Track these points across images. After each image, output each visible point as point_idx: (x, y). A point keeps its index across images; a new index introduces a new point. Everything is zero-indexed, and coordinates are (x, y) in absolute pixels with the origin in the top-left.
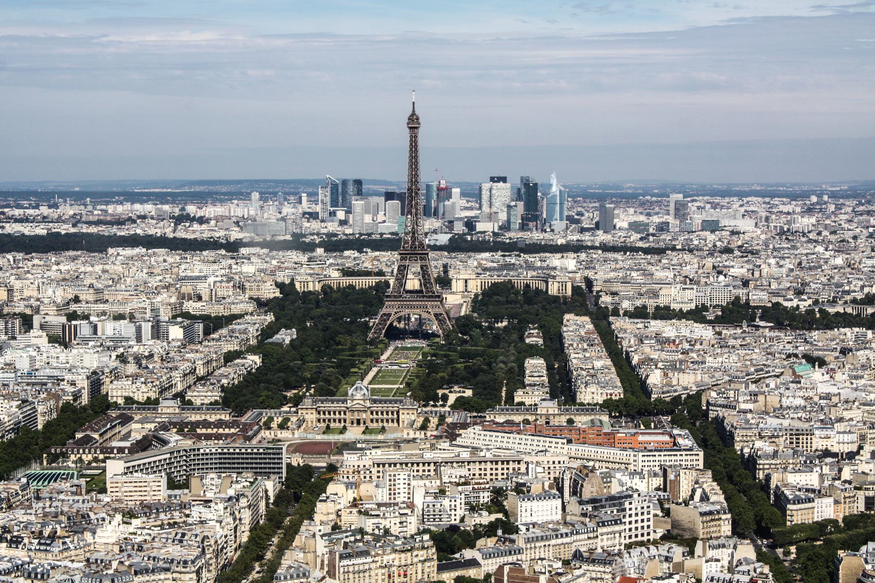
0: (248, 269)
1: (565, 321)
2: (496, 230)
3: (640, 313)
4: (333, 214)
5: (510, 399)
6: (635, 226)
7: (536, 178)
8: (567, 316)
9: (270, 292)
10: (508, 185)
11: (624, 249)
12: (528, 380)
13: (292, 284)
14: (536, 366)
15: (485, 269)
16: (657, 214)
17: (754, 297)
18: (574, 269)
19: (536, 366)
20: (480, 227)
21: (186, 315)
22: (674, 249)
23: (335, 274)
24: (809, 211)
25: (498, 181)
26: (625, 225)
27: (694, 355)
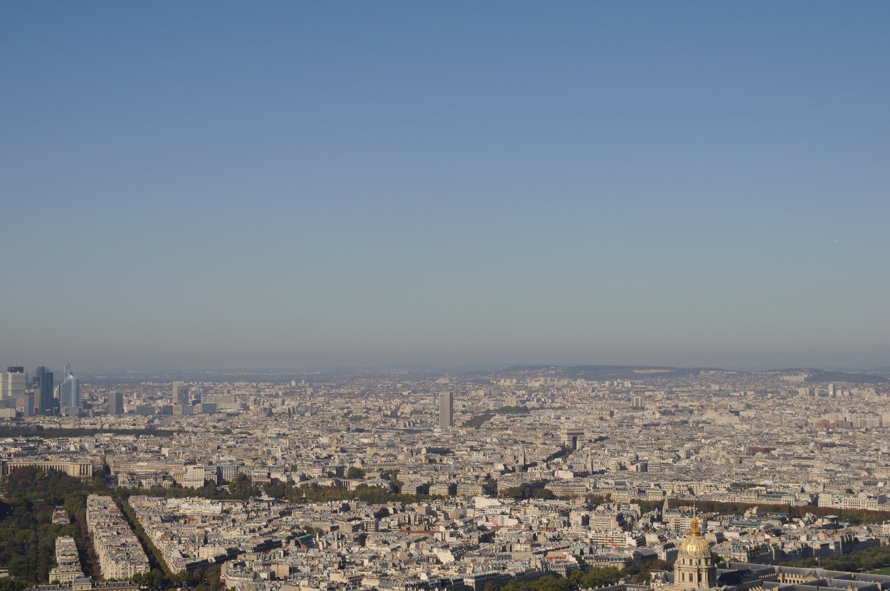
1: (88, 501)
2: (14, 416)
3: (158, 492)
5: (47, 578)
6: (143, 411)
7: (51, 368)
8: (91, 497)
10: (24, 374)
11: (137, 433)
12: (59, 559)
14: (65, 545)
15: (10, 455)
16: (161, 398)
17: (256, 474)
18: (94, 451)
19: (65, 545)
22: (179, 432)
24: (290, 393)
25: (15, 371)
27: (209, 529)
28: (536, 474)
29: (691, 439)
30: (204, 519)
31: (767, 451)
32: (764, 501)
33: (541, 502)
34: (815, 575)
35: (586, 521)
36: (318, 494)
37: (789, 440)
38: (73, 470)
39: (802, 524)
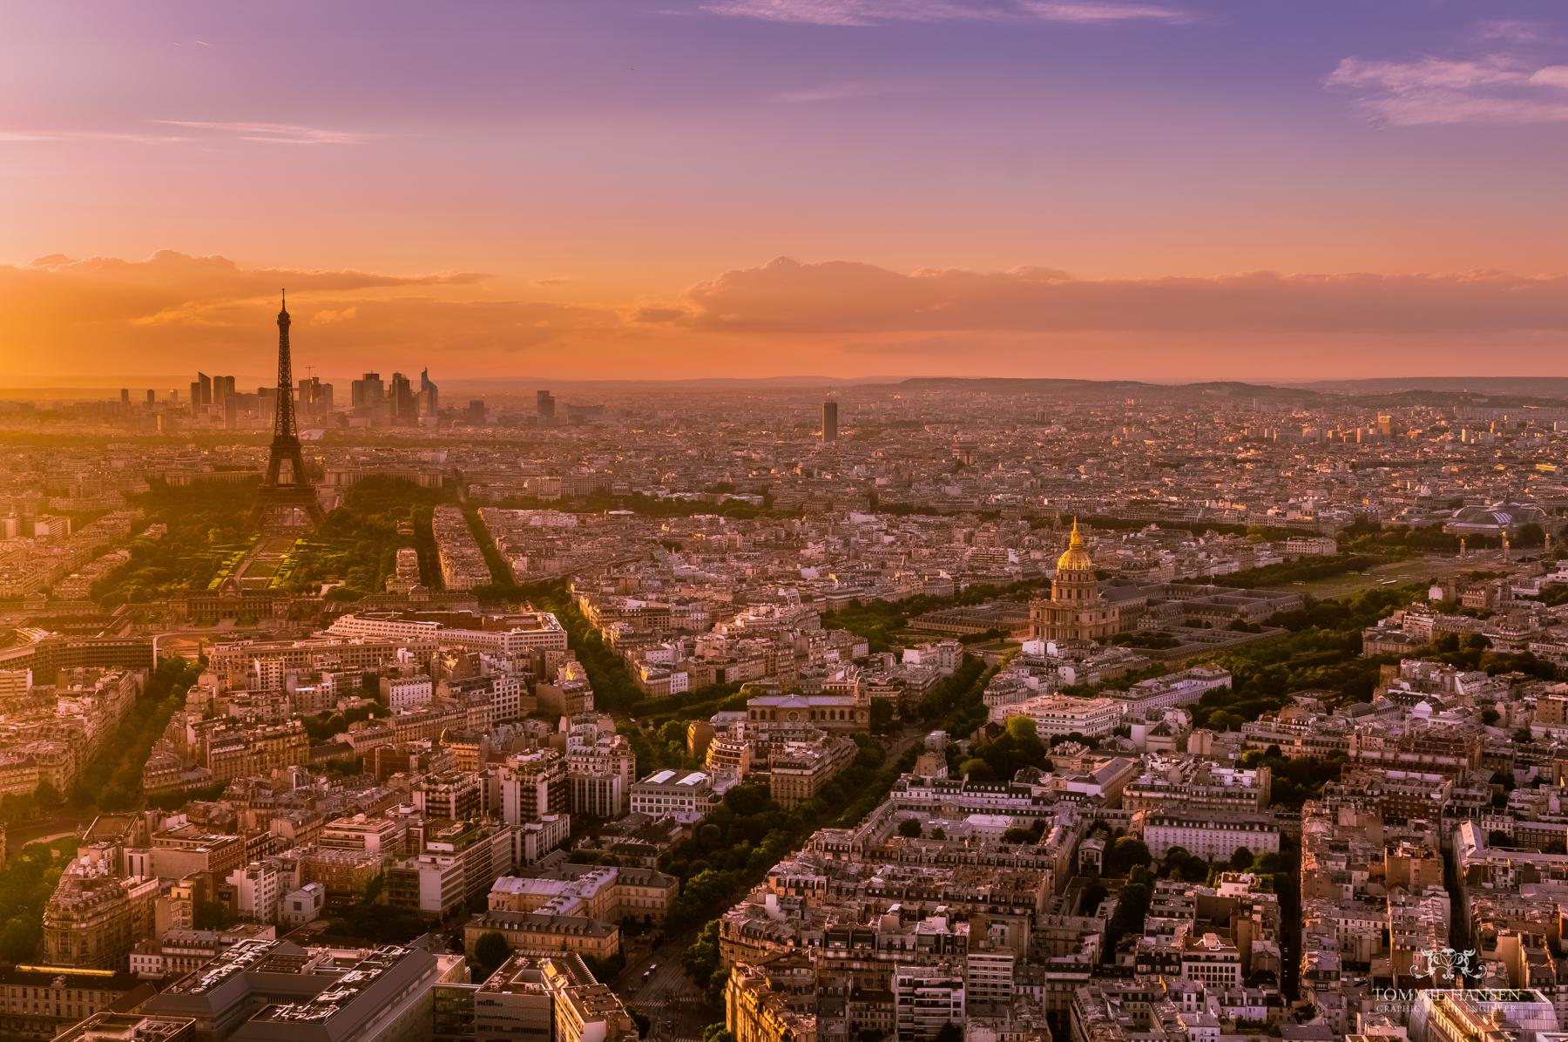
0: (118, 464)
3: (510, 503)
4: (205, 410)
6: (505, 421)
9: (142, 488)
13: (163, 478)
20: (353, 422)
21: (55, 512)
23: (207, 469)
26: (495, 420)
28: (922, 492)
29: (1095, 455)
30: (556, 530)
31: (1176, 467)
32: (1166, 518)
33: (921, 518)
34: (1207, 592)
35: (969, 539)
36: (683, 509)
37: (1199, 453)
38: (424, 480)
39: (1202, 541)
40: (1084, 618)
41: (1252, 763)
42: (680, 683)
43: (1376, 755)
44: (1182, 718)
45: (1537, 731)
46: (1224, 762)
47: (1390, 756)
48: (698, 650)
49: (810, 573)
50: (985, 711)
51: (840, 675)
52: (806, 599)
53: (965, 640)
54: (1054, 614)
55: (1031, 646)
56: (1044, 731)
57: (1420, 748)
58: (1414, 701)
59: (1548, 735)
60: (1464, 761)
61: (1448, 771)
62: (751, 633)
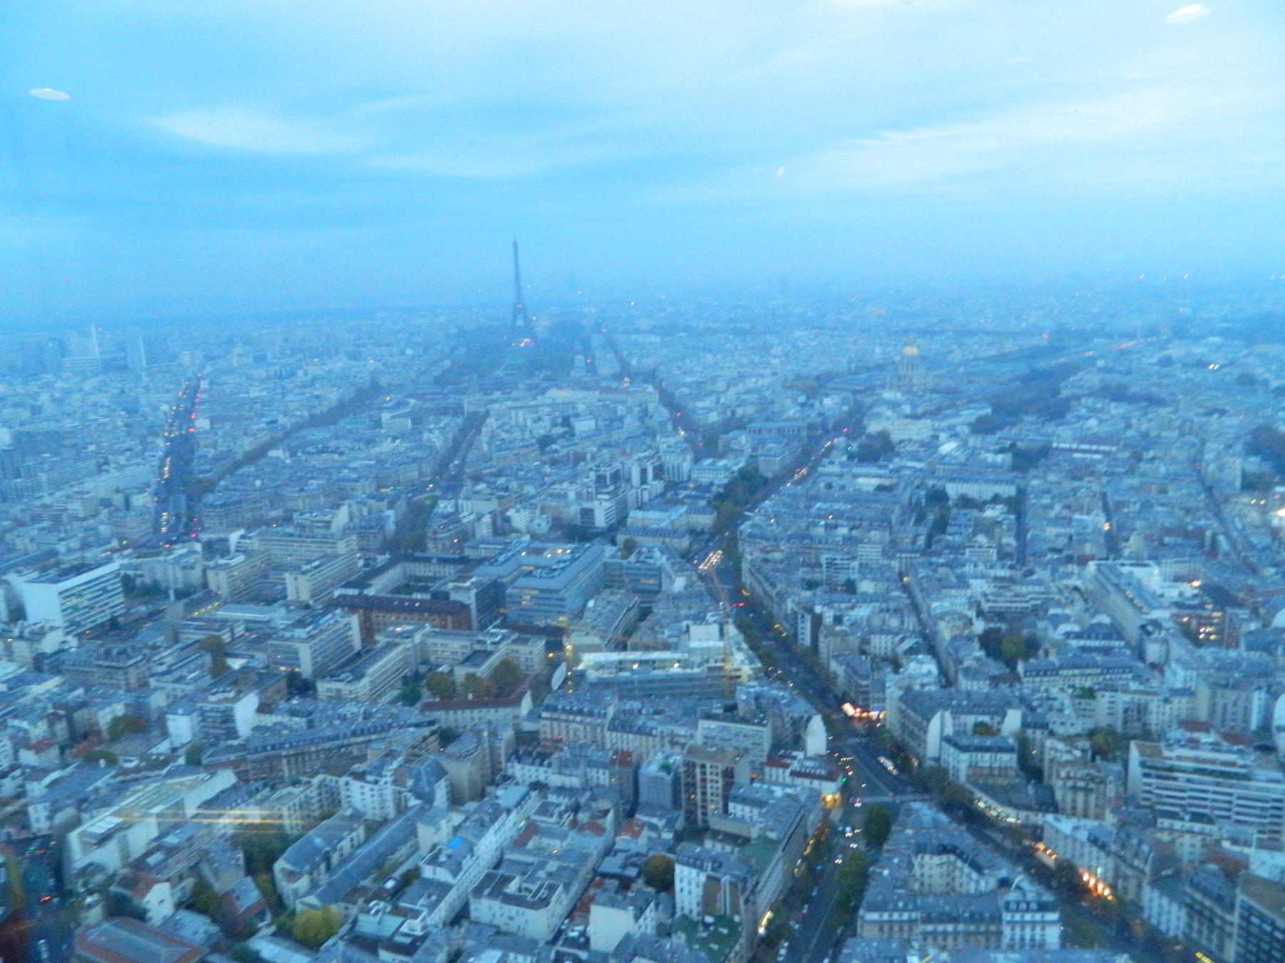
19: (579, 358)
30: (651, 344)
40: (915, 381)
41: (1002, 451)
42: (713, 417)
43: (1067, 446)
44: (966, 429)
45: (1154, 433)
46: (988, 451)
47: (1074, 446)
48: (722, 401)
49: (775, 362)
50: (865, 428)
51: (792, 412)
52: (774, 374)
53: (855, 392)
54: (900, 378)
55: (888, 395)
56: (895, 437)
57: (1091, 443)
58: (1088, 418)
59: (1159, 436)
60: (1114, 449)
61: (1106, 453)
62: (748, 392)
